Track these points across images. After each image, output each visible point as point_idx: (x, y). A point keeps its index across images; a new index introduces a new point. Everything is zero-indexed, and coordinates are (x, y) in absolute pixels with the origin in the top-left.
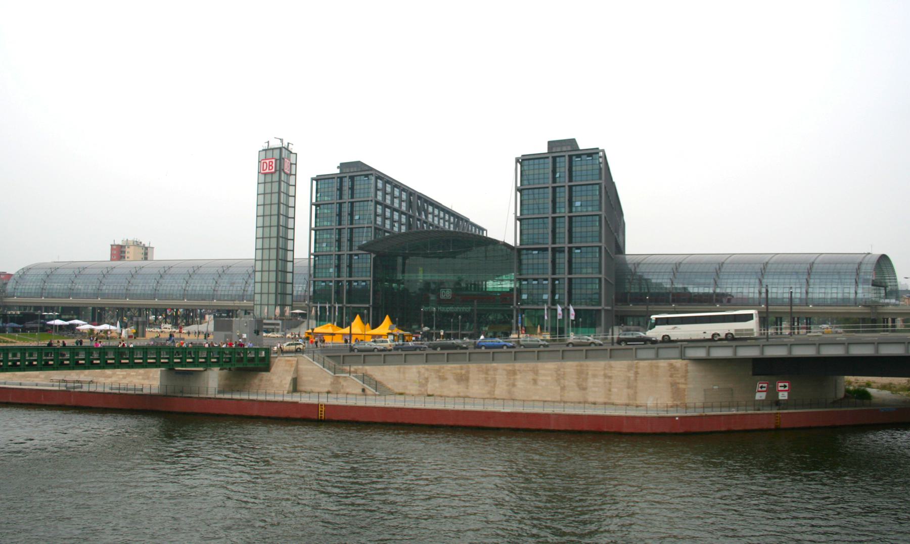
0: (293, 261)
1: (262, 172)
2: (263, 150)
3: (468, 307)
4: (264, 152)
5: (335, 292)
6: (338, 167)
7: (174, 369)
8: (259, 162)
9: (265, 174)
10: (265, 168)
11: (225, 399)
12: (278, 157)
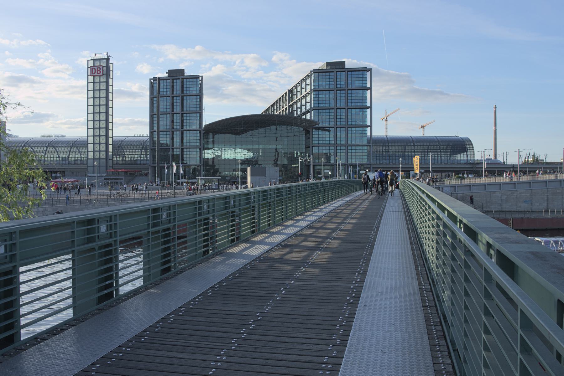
0: (112, 137)
1: (91, 75)
2: (92, 60)
4: (93, 61)
8: (88, 68)
10: (94, 72)
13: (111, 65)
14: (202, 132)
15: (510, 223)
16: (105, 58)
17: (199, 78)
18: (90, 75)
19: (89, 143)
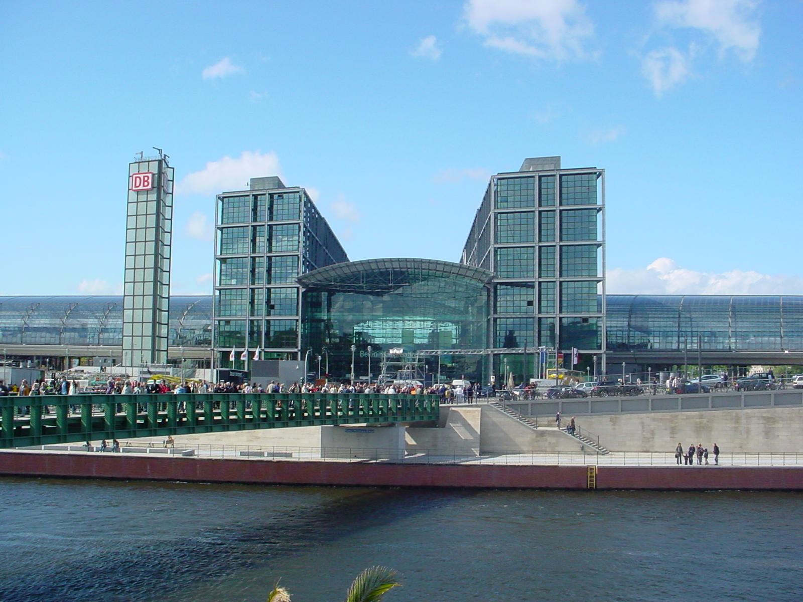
0: (168, 298)
1: (134, 188)
2: (136, 163)
3: (393, 354)
5: (265, 334)
7: (338, 426)
8: (129, 176)
9: (138, 192)
10: (137, 185)
11: (447, 465)
12: (156, 172)
15: (593, 477)
16: (157, 159)
18: (132, 189)
19: (125, 308)
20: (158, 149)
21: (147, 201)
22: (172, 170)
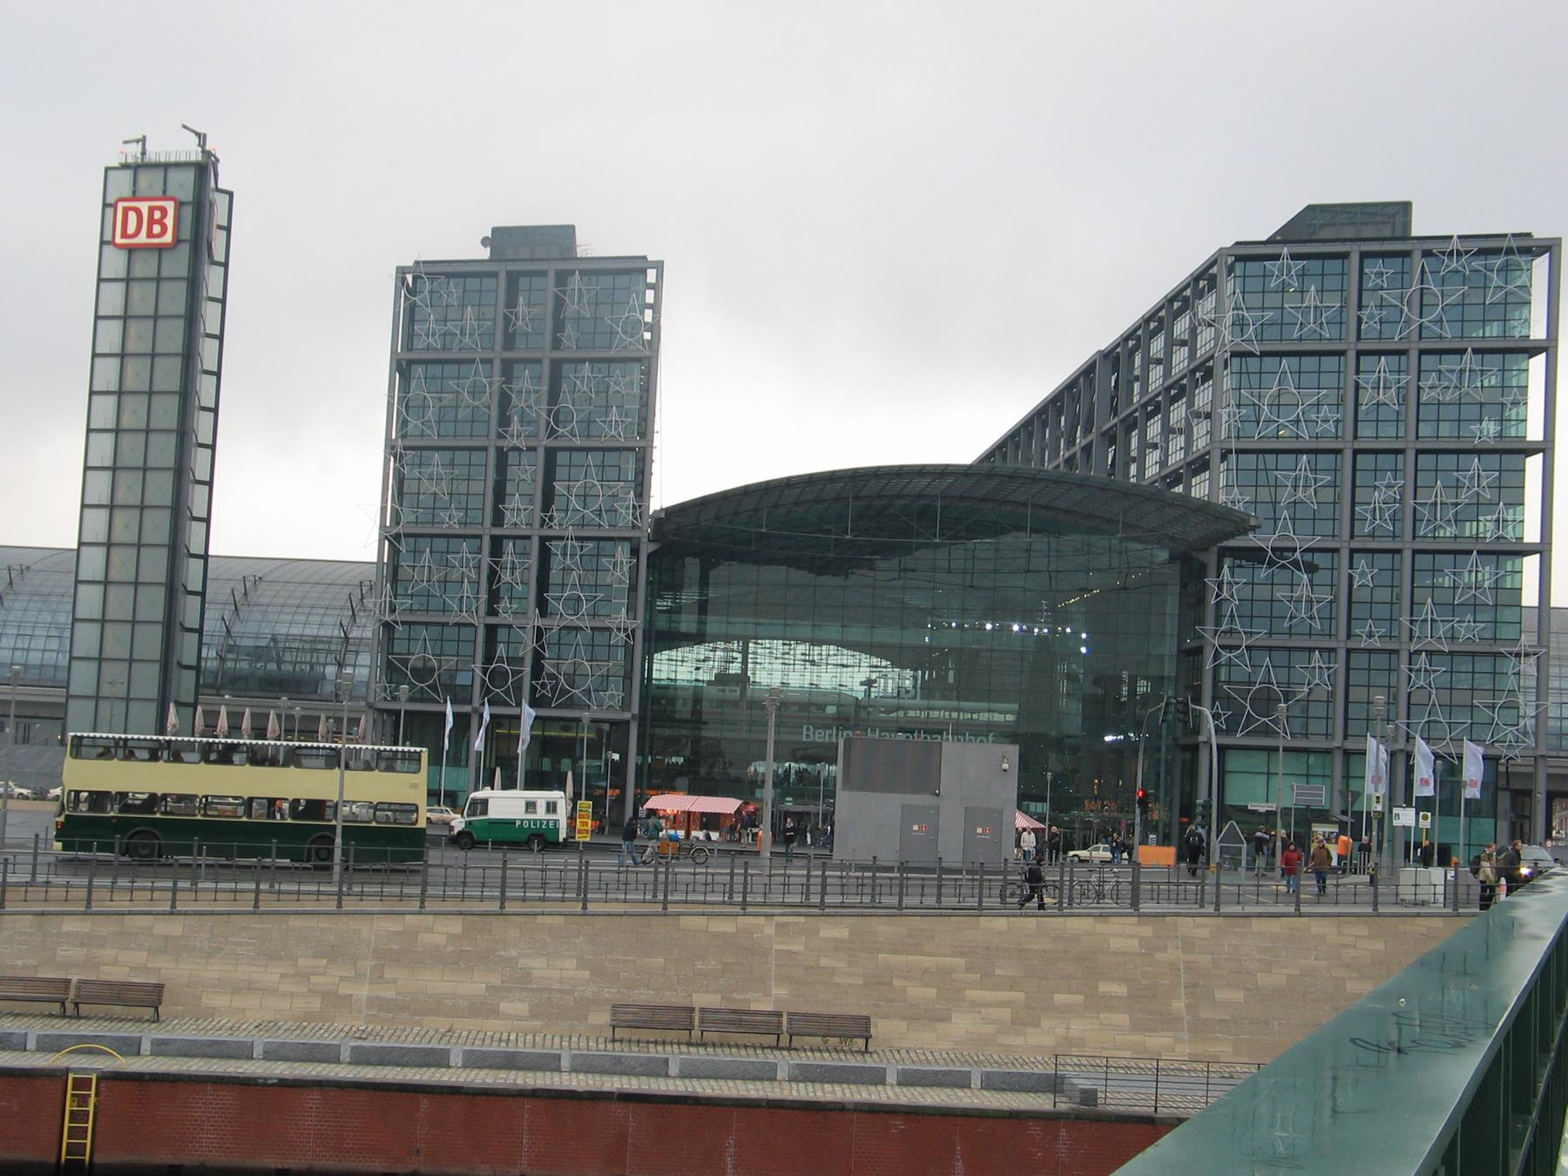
1: (119, 240)
2: (125, 166)
4: (128, 174)
6: (485, 242)
8: (105, 205)
9: (131, 250)
10: (131, 229)
12: (187, 194)
13: (221, 202)
14: (646, 548)
16: (193, 159)
17: (644, 272)
18: (112, 242)
20: (198, 135)
21: (159, 280)
22: (227, 197)
